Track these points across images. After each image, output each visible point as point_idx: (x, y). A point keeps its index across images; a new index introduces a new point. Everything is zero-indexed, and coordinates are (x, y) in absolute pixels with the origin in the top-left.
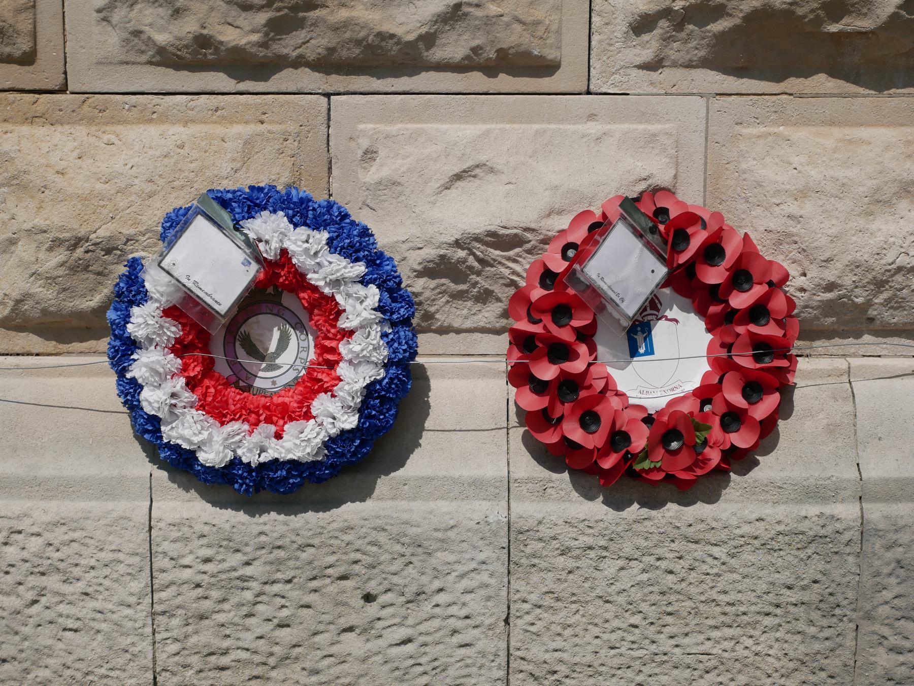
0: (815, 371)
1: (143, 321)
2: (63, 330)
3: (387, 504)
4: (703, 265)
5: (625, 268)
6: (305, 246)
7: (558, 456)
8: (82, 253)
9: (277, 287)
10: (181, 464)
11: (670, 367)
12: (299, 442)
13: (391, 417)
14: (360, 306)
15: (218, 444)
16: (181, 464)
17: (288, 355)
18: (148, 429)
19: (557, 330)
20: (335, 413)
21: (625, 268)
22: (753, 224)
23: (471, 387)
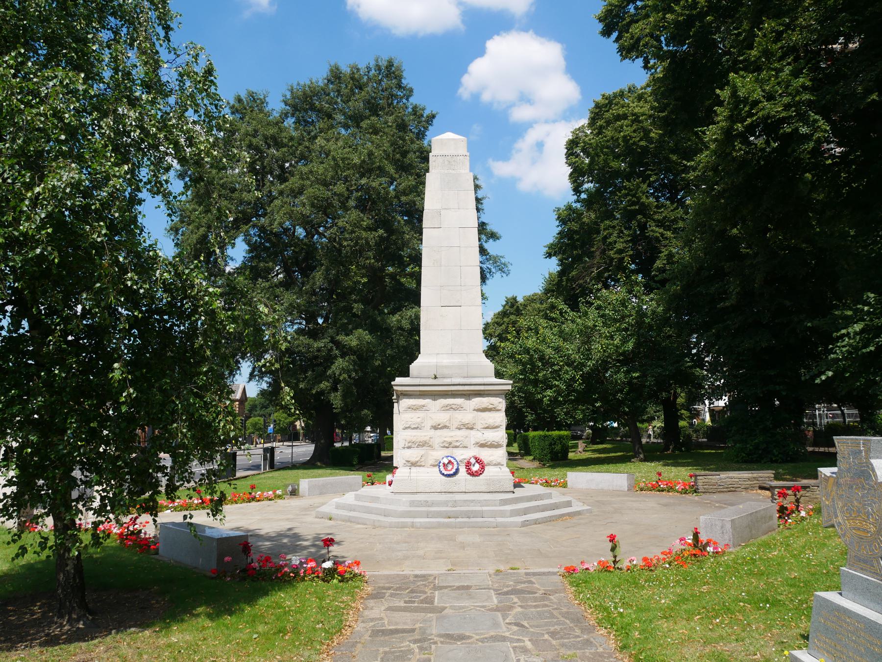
0: (486, 468)
1: (441, 464)
2: (434, 466)
3: (457, 477)
4: (478, 460)
5: (473, 461)
6: (452, 460)
7: (469, 474)
8: (436, 460)
9: (450, 462)
10: (443, 474)
11: (476, 468)
12: (451, 472)
13: (457, 471)
14: (455, 463)
15: (446, 473)
16: (443, 474)
17: (450, 467)
18: (441, 472)
19: (468, 465)
20: (454, 470)
21: (473, 461)
22: (481, 458)
23: (463, 469)
